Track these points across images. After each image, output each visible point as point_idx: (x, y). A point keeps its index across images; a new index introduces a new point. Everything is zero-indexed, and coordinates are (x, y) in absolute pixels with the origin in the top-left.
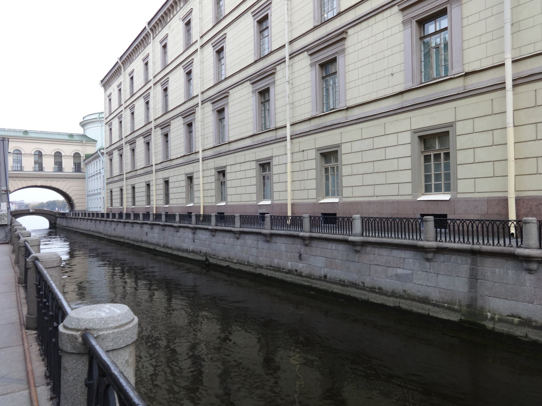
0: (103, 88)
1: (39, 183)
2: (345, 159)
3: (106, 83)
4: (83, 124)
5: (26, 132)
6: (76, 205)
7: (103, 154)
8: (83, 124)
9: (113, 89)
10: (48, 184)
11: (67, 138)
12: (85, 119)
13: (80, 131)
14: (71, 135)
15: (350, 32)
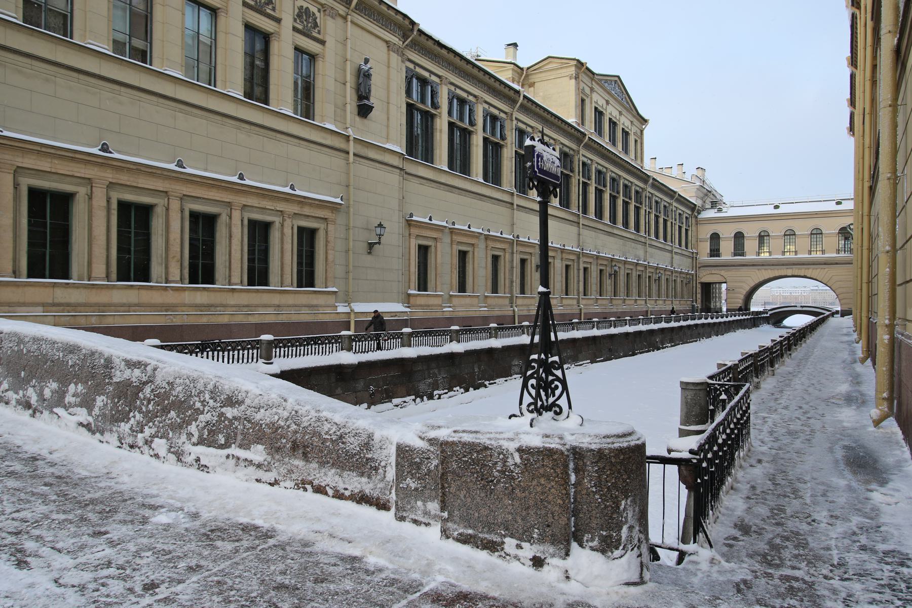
1: (789, 272)
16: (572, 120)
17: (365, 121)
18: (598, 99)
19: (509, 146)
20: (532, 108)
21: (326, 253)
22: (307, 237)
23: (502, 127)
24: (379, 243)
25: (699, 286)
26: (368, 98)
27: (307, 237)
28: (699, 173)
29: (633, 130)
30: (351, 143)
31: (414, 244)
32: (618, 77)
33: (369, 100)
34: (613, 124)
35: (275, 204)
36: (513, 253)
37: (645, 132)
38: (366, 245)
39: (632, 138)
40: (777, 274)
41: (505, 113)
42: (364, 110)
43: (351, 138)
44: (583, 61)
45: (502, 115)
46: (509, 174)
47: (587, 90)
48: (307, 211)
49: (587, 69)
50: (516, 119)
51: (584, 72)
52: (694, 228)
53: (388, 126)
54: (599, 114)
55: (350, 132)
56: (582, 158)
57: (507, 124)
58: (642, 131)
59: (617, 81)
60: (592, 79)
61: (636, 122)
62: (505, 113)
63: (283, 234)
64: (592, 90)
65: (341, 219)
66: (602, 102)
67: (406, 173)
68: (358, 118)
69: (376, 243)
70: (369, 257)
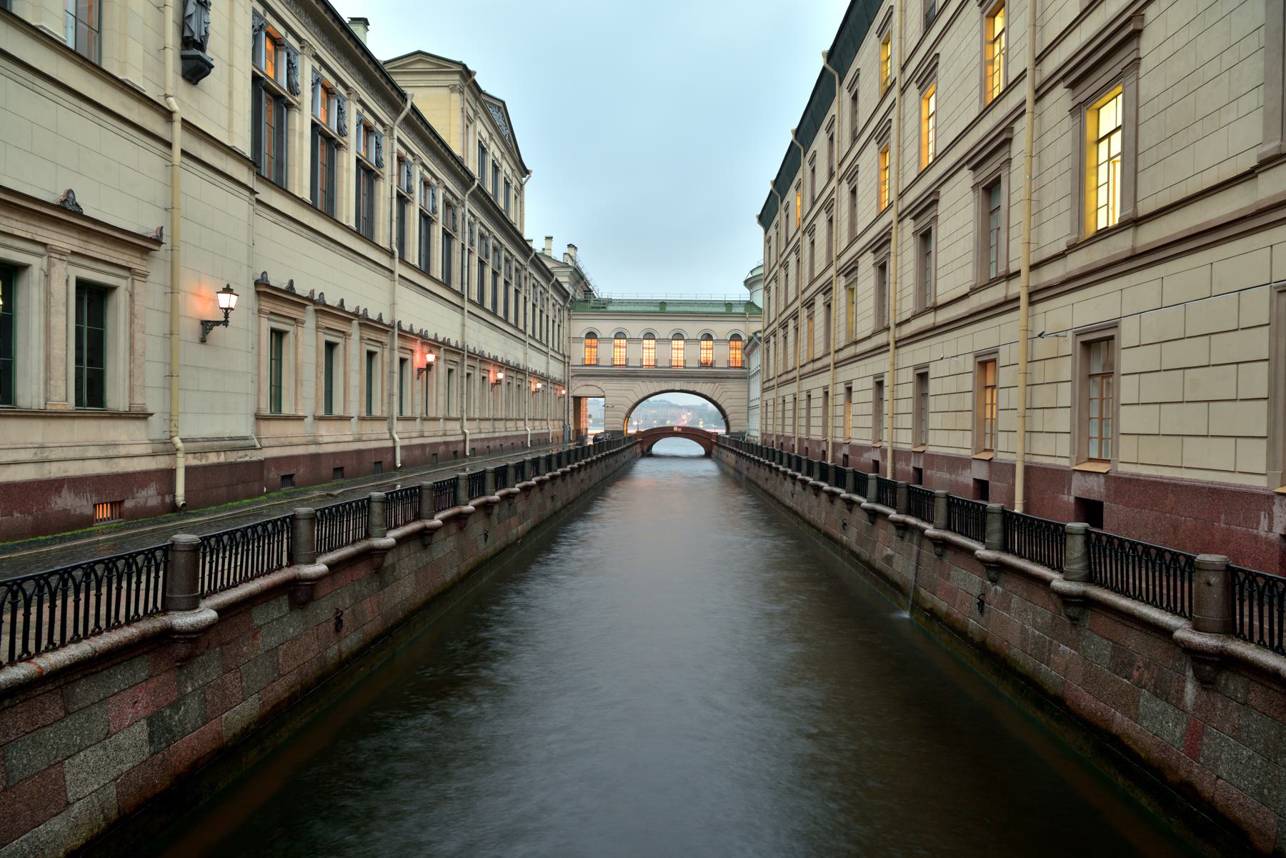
0: (761, 230)
1: (678, 385)
2: (1127, 361)
3: (766, 218)
4: (749, 283)
5: (663, 304)
6: (731, 423)
7: (760, 339)
8: (749, 283)
9: (772, 231)
10: (691, 387)
11: (723, 310)
12: (755, 273)
13: (744, 294)
14: (729, 305)
15: (943, 190)
16: (457, 151)
17: (194, 88)
18: (481, 129)
19: (387, 178)
20: (418, 125)
21: (132, 337)
22: (93, 299)
23: (378, 146)
24: (226, 323)
25: (571, 400)
26: (201, 46)
27: (93, 299)
28: (572, 252)
29: (514, 183)
30: (177, 126)
31: (266, 325)
32: (503, 103)
33: (203, 50)
34: (496, 169)
35: (32, 229)
36: (392, 349)
37: (526, 187)
38: (197, 326)
39: (512, 192)
40: (665, 386)
41: (383, 124)
42: (195, 69)
43: (177, 117)
44: (470, 67)
45: (379, 127)
46: (388, 224)
47: (471, 113)
48: (96, 249)
49: (475, 82)
50: (399, 140)
51: (469, 86)
52: (566, 324)
53: (230, 109)
54: (483, 150)
55: (173, 104)
56: (468, 215)
57: (385, 142)
58: (522, 186)
59: (502, 106)
60: (477, 99)
61: (517, 173)
62: (383, 124)
63: (48, 293)
64: (476, 112)
65: (156, 268)
66: (485, 135)
67: (258, 201)
68: (181, 81)
69: (218, 323)
70: (202, 346)
